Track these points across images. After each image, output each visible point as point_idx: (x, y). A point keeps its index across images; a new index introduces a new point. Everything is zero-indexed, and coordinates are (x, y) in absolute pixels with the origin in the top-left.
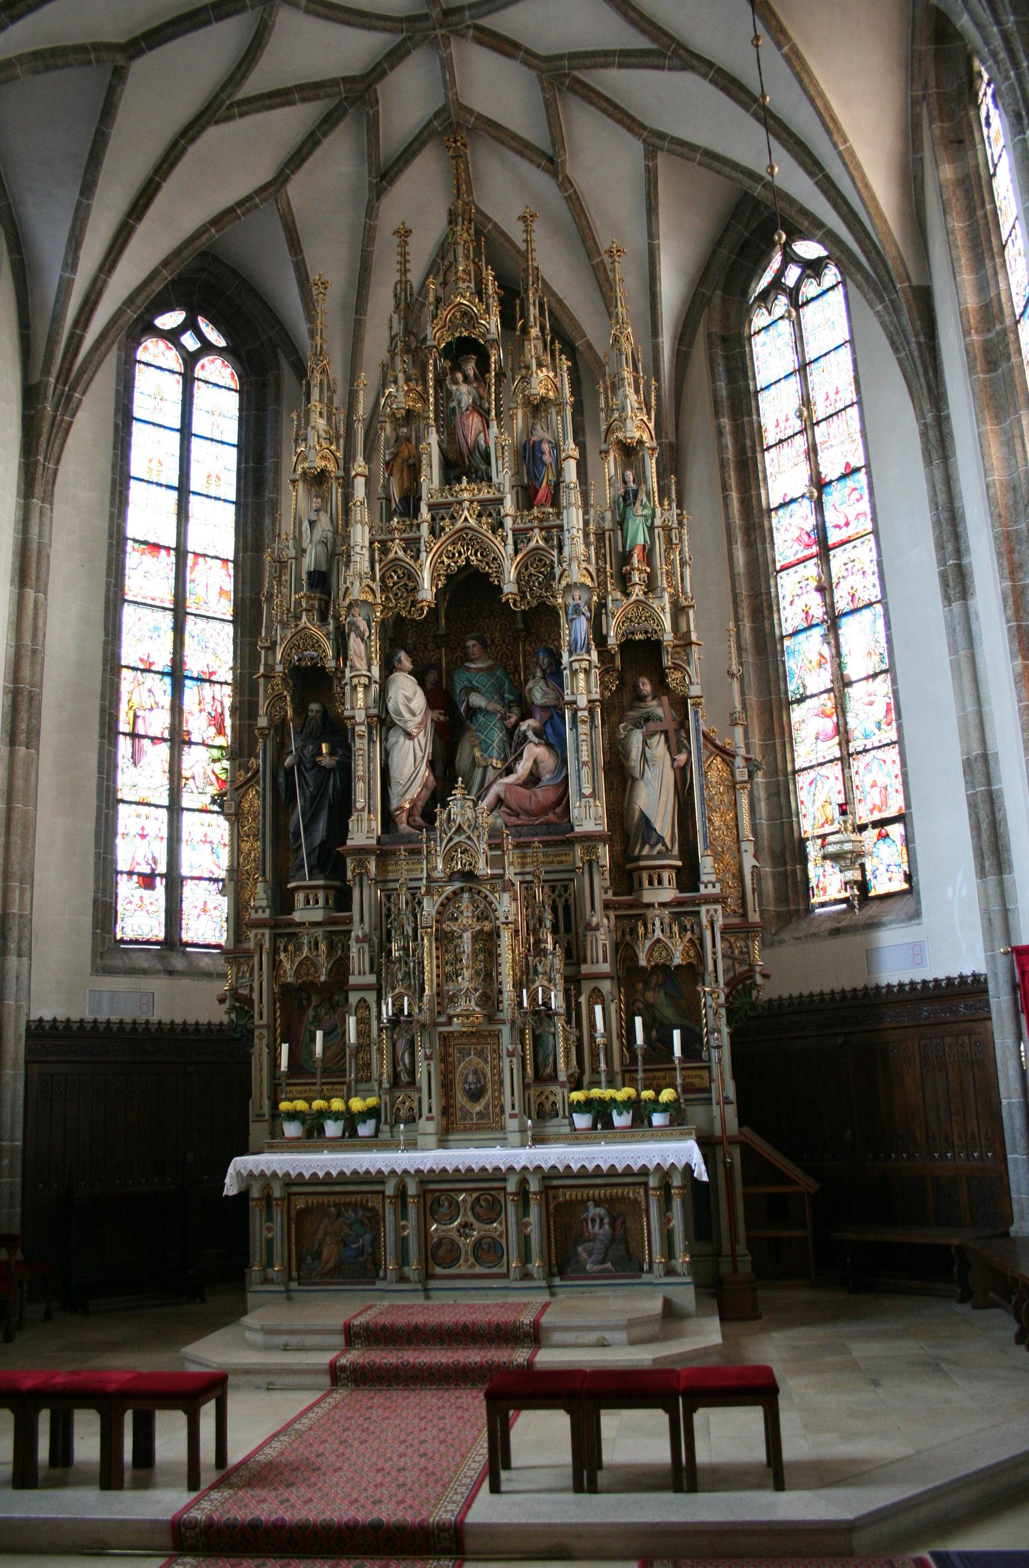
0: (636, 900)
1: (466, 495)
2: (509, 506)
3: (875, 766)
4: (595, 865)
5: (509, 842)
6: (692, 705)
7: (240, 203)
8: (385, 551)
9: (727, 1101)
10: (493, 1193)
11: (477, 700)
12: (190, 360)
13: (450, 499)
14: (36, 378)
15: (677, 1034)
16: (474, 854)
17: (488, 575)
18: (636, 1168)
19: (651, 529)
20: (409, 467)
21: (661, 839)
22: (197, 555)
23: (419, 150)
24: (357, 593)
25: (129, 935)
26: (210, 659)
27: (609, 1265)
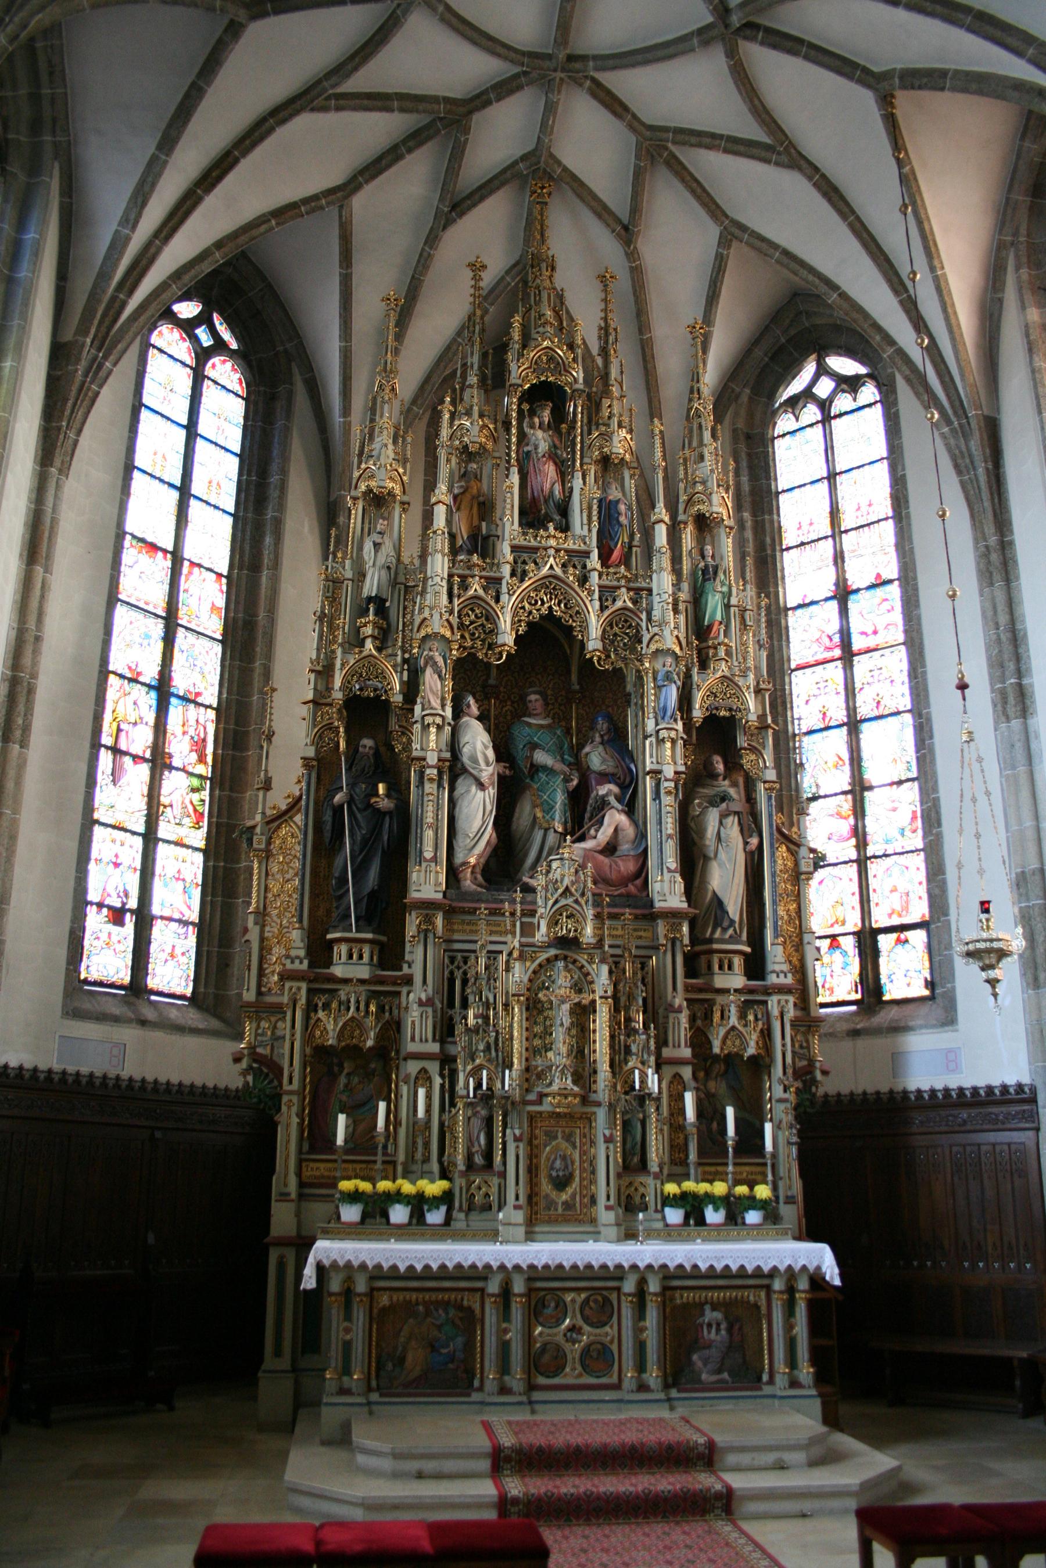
0: (705, 984)
1: (552, 542)
2: (594, 561)
3: (896, 871)
4: (678, 943)
6: (766, 789)
7: (306, 201)
8: (464, 586)
10: (605, 1293)
11: (541, 757)
12: (203, 355)
13: (533, 543)
14: (68, 335)
16: (581, 919)
17: (571, 628)
18: (766, 1269)
19: (727, 606)
20: (479, 504)
22: (193, 564)
23: (492, 192)
24: (437, 625)
25: (94, 975)
26: (196, 677)
27: (725, 1375)
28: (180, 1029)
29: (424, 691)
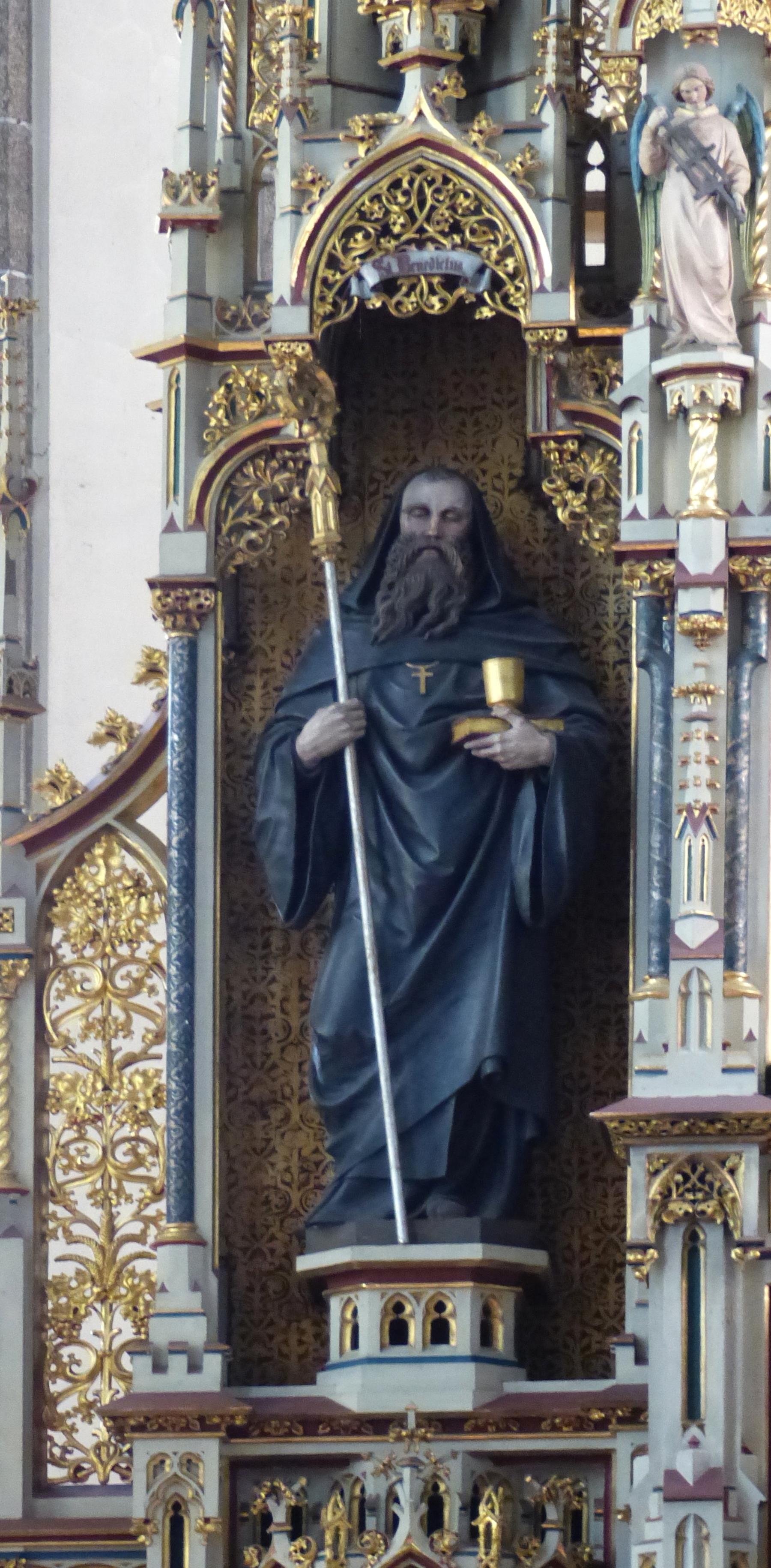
29: (658, 272)
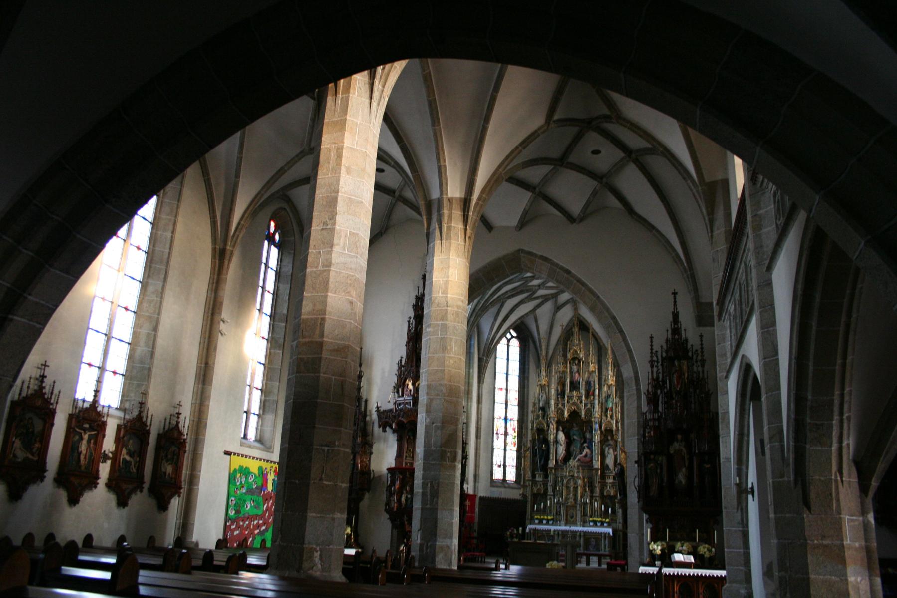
2: (583, 398)
5: (580, 468)
7: (525, 315)
8: (557, 405)
9: (620, 523)
11: (575, 437)
12: (509, 341)
14: (481, 356)
15: (610, 509)
21: (610, 470)
28: (513, 488)
